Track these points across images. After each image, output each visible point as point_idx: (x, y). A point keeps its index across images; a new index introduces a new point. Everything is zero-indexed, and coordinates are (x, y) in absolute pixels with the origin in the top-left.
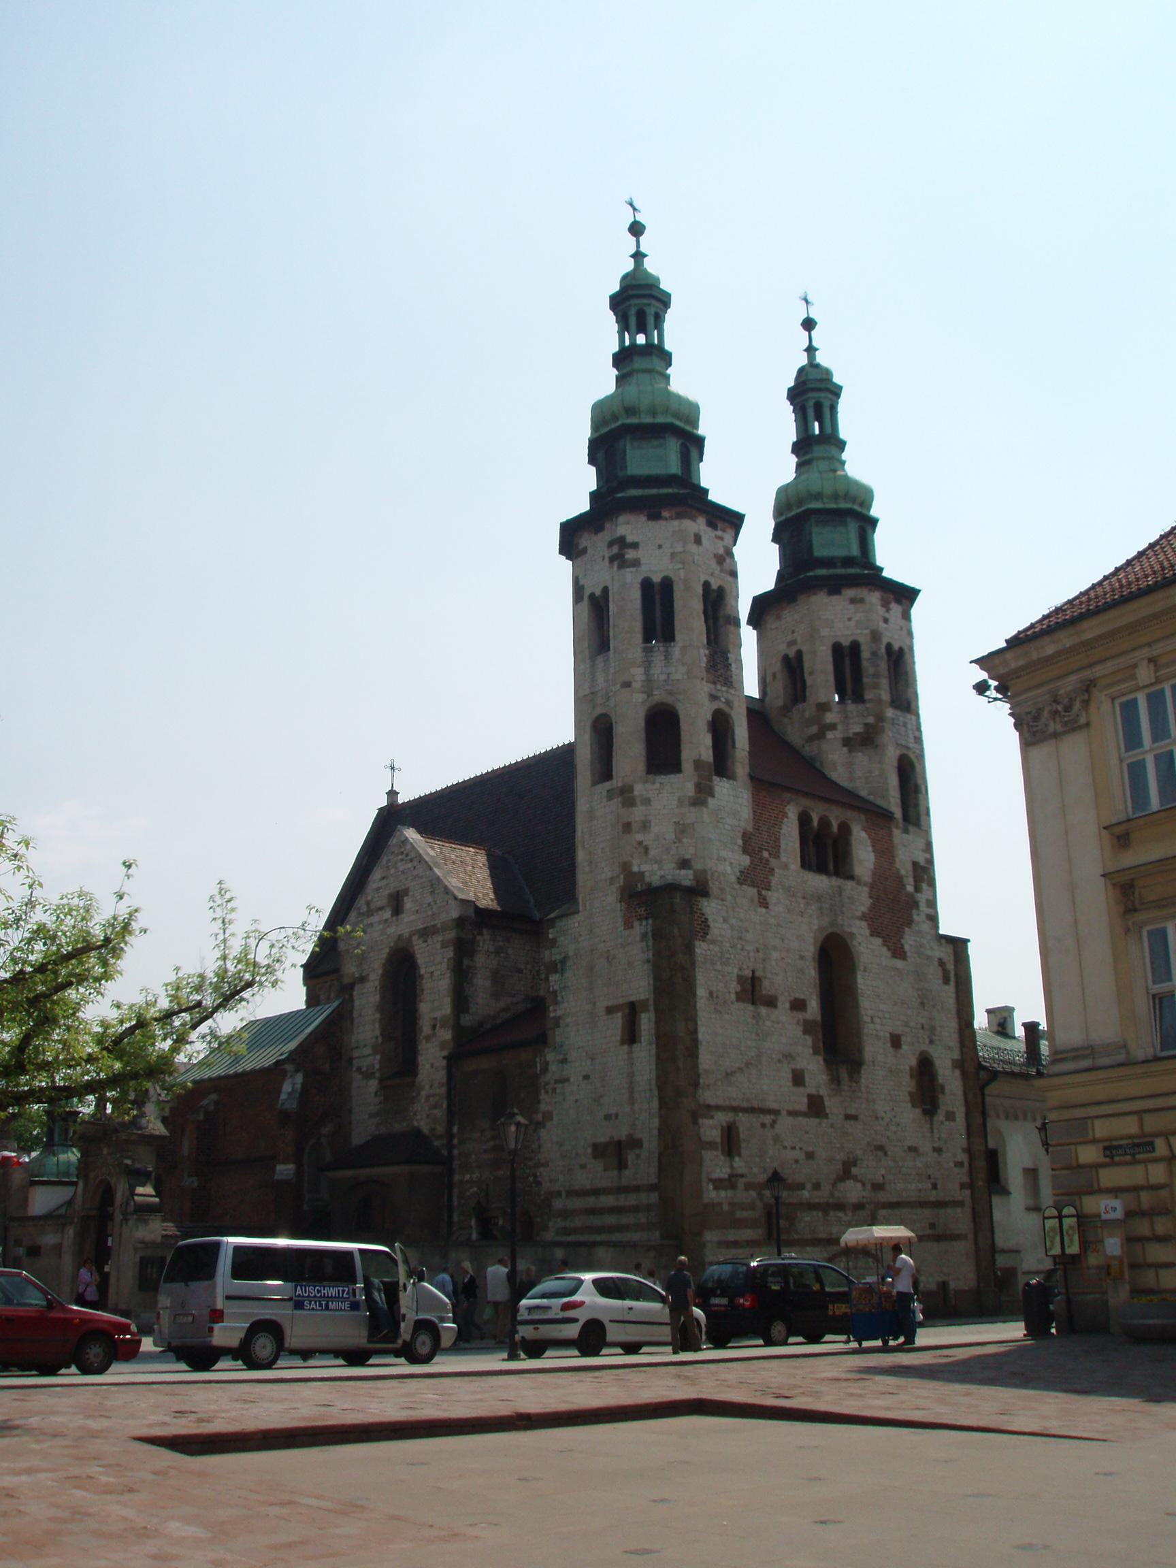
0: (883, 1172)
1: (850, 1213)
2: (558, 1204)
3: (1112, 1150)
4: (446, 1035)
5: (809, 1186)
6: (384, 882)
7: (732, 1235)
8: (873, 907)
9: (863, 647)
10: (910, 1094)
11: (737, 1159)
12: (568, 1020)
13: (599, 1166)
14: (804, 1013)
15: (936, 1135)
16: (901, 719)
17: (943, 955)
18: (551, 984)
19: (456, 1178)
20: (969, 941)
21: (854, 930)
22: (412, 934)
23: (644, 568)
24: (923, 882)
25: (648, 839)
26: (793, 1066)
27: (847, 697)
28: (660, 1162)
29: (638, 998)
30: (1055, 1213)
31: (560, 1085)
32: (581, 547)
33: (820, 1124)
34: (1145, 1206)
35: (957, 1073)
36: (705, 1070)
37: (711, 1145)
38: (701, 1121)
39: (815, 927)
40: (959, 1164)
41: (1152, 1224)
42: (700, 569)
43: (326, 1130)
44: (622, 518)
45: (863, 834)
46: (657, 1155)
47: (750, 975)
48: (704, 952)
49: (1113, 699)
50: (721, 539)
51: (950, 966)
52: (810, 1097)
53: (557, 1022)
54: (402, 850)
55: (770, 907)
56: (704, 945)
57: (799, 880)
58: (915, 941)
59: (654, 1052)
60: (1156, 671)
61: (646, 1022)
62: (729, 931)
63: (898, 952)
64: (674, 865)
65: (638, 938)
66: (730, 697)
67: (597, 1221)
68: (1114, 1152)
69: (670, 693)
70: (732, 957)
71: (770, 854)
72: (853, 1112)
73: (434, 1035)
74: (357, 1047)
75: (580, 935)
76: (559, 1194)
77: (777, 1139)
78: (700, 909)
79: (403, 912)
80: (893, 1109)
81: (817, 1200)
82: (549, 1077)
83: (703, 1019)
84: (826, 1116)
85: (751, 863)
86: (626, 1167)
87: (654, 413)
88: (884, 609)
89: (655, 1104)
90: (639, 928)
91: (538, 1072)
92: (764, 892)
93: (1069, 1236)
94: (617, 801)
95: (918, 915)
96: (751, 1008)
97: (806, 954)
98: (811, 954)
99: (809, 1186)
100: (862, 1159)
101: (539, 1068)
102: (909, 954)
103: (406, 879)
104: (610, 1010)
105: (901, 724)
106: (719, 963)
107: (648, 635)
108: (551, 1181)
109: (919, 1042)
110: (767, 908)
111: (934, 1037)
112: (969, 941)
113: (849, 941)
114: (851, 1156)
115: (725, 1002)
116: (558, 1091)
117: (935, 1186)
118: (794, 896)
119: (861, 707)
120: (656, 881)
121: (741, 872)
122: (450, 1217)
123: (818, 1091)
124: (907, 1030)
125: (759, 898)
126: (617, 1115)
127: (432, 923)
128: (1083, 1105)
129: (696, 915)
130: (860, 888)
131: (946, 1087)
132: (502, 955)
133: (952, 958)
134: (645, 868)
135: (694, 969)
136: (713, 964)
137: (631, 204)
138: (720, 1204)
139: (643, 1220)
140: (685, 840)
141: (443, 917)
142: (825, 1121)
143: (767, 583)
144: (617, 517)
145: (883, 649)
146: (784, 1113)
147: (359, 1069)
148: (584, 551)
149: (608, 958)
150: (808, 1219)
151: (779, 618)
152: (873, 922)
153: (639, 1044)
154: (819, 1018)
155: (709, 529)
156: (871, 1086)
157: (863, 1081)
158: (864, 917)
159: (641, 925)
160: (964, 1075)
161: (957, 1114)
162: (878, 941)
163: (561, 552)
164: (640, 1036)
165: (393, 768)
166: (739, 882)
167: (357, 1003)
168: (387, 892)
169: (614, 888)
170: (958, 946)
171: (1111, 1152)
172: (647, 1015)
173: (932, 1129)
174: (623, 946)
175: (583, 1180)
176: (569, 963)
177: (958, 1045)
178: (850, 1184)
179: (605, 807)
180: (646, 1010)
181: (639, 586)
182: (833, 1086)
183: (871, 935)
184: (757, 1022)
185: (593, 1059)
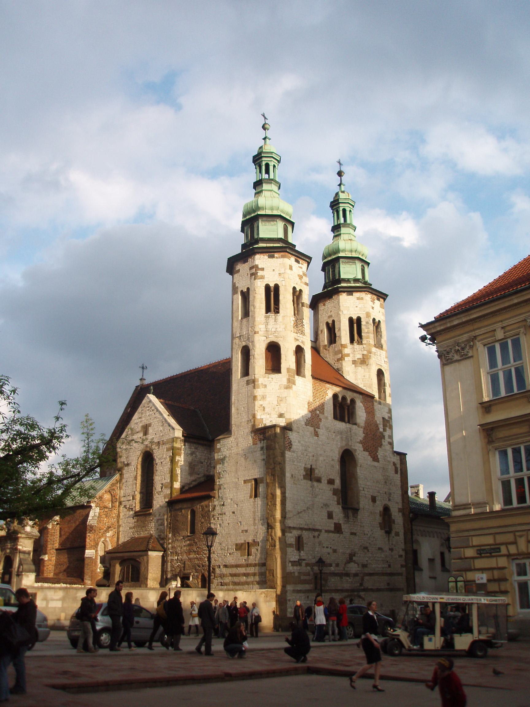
0: (367, 559)
1: (352, 578)
2: (218, 571)
3: (482, 552)
4: (169, 492)
5: (334, 565)
6: (140, 420)
7: (299, 587)
8: (365, 438)
9: (362, 320)
10: (380, 523)
11: (302, 552)
12: (225, 486)
13: (239, 553)
14: (333, 485)
15: (391, 543)
16: (379, 352)
17: (395, 461)
20: (407, 454)
21: (356, 448)
24: (387, 427)
25: (264, 403)
26: (328, 510)
27: (354, 342)
30: (453, 579)
31: (221, 516)
32: (237, 269)
33: (339, 536)
34: (496, 577)
35: (401, 514)
36: (289, 511)
37: (291, 545)
38: (286, 534)
39: (339, 446)
40: (401, 556)
41: (499, 585)
42: (291, 281)
43: (108, 534)
44: (257, 256)
45: (361, 404)
47: (310, 467)
48: (289, 456)
49: (484, 345)
50: (301, 268)
51: (398, 466)
52: (335, 524)
54: (149, 405)
55: (319, 436)
56: (289, 452)
57: (332, 424)
58: (383, 454)
60: (504, 333)
62: (301, 447)
63: (375, 459)
65: (259, 449)
66: (304, 340)
67: (236, 579)
68: (482, 552)
70: (302, 458)
71: (320, 412)
72: (355, 531)
73: (162, 491)
74: (124, 496)
75: (232, 447)
77: (320, 543)
78: (289, 437)
80: (372, 530)
81: (336, 572)
82: (215, 512)
83: (288, 487)
84: (342, 533)
85: (312, 416)
87: (272, 209)
88: (372, 303)
92: (317, 429)
93: (460, 590)
95: (384, 442)
96: (310, 482)
97: (335, 458)
98: (337, 458)
99: (334, 565)
100: (358, 553)
102: (380, 460)
103: (151, 419)
104: (245, 482)
105: (379, 355)
106: (296, 461)
107: (268, 310)
109: (384, 500)
110: (318, 437)
111: (391, 498)
112: (407, 454)
113: (354, 453)
114: (353, 551)
115: (298, 479)
117: (389, 566)
118: (330, 432)
119: (361, 346)
120: (268, 424)
121: (307, 420)
123: (339, 521)
124: (379, 494)
125: (314, 432)
127: (162, 440)
128: (467, 531)
129: (286, 439)
130: (359, 429)
131: (396, 521)
132: (194, 455)
133: (399, 462)
135: (285, 464)
136: (293, 462)
137: (264, 116)
138: (294, 572)
140: (282, 404)
142: (342, 535)
143: (319, 290)
145: (371, 321)
146: (323, 531)
148: (239, 271)
150: (333, 580)
151: (324, 305)
152: (364, 444)
154: (340, 488)
155: (296, 263)
156: (362, 519)
157: (359, 517)
158: (361, 442)
159: (261, 443)
160: (404, 515)
161: (400, 533)
162: (367, 453)
163: (227, 272)
165: (143, 368)
166: (306, 425)
168: (141, 425)
170: (402, 456)
171: (480, 552)
172: (263, 484)
173: (389, 539)
175: (231, 560)
176: (227, 459)
177: (401, 501)
178: (352, 565)
181: (264, 288)
182: (345, 519)
183: (364, 450)
184: (312, 490)
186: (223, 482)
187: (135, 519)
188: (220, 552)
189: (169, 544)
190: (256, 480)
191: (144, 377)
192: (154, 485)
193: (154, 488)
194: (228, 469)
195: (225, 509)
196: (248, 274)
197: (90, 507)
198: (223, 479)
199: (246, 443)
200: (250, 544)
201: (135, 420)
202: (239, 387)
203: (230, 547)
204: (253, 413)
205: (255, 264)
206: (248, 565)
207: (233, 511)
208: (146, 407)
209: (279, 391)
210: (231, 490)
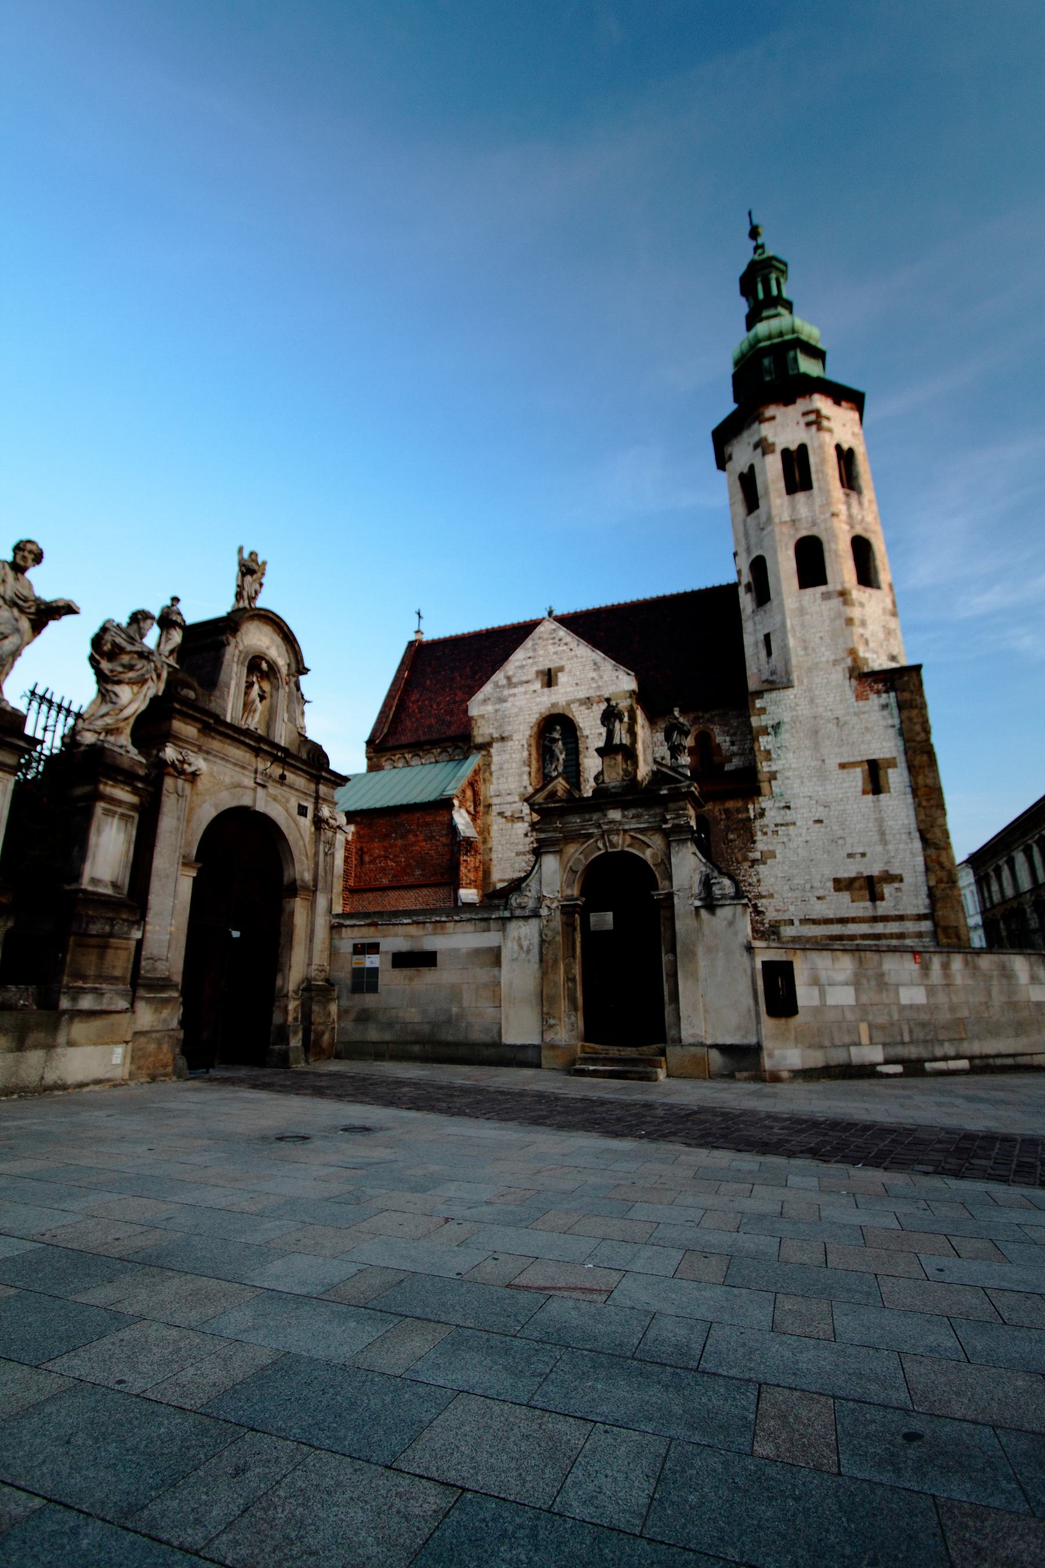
2: (787, 932)
6: (530, 661)
13: (845, 897)
22: (568, 704)
25: (867, 634)
28: (931, 894)
29: (882, 756)
31: (783, 828)
46: (926, 888)
53: (773, 776)
61: (897, 778)
65: (876, 708)
69: (866, 530)
76: (791, 922)
79: (557, 684)
82: (765, 821)
86: (882, 899)
89: (918, 845)
90: (875, 701)
91: (752, 817)
94: (836, 602)
101: (752, 815)
104: (843, 766)
108: (777, 911)
116: (779, 833)
126: (863, 855)
134: (868, 655)
144: (810, 396)
147: (501, 814)
148: (773, 418)
149: (838, 725)
153: (888, 794)
164: (889, 788)
165: (420, 617)
167: (495, 759)
168: (535, 669)
169: (839, 668)
172: (895, 770)
174: (855, 714)
176: (783, 728)
179: (820, 605)
180: (895, 766)
186: (781, 767)
187: (532, 836)
188: (789, 895)
191: (422, 629)
193: (582, 779)
194: (793, 743)
195: (789, 816)
197: (453, 805)
199: (838, 698)
200: (875, 879)
201: (517, 660)
202: (803, 603)
203: (817, 884)
204: (850, 646)
206: (875, 919)
207: (816, 818)
208: (547, 639)
209: (882, 617)
210: (805, 780)
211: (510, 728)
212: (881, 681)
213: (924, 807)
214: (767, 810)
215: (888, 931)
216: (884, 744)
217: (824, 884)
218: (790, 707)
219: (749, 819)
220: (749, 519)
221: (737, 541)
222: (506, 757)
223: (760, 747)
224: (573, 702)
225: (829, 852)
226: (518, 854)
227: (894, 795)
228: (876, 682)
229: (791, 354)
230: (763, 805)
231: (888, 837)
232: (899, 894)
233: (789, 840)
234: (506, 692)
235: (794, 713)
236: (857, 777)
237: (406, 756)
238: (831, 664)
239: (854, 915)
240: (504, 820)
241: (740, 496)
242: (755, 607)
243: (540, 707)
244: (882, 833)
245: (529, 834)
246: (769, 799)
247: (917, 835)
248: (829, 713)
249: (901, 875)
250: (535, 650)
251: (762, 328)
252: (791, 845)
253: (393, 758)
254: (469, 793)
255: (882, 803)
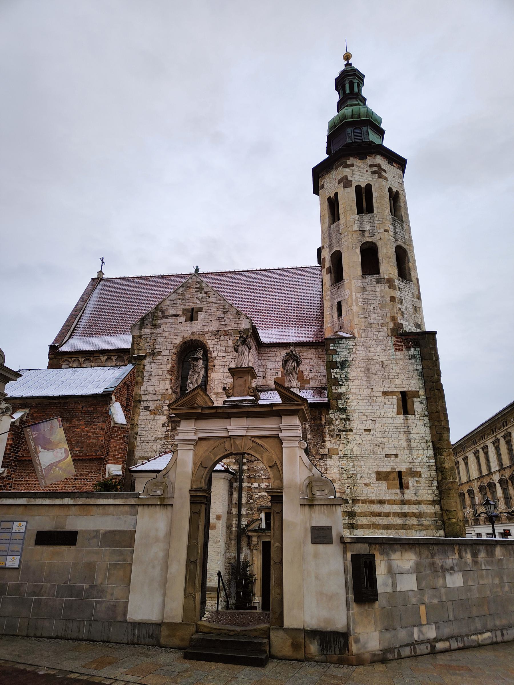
6: (180, 301)
12: (347, 396)
13: (383, 485)
18: (332, 374)
19: (245, 485)
23: (389, 182)
25: (403, 308)
29: (410, 390)
31: (344, 433)
44: (378, 157)
46: (436, 482)
59: (427, 421)
64: (414, 325)
65: (407, 357)
75: (357, 350)
79: (197, 320)
86: (408, 488)
89: (431, 451)
91: (324, 424)
104: (385, 394)
116: (342, 436)
120: (408, 331)
122: (240, 510)
126: (396, 456)
134: (402, 323)
139: (427, 523)
141: (235, 327)
144: (375, 156)
148: (352, 165)
165: (103, 263)
168: (183, 307)
172: (419, 400)
185: (372, 421)
186: (345, 391)
187: (168, 426)
189: (244, 464)
190: (404, 394)
192: (209, 383)
193: (208, 387)
194: (353, 375)
196: (367, 171)
197: (111, 400)
198: (343, 387)
199: (383, 348)
200: (403, 474)
204: (393, 315)
205: (377, 163)
206: (403, 502)
207: (367, 428)
209: (412, 299)
211: (159, 346)
212: (411, 340)
213: (436, 426)
214: (334, 419)
215: (410, 511)
216: (413, 382)
217: (370, 475)
218: (353, 351)
219: (321, 425)
220: (332, 226)
221: (323, 239)
222: (155, 367)
223: (331, 375)
224: (207, 332)
225: (374, 452)
226: (157, 439)
227: (417, 416)
228: (407, 339)
229: (365, 129)
230: (332, 416)
231: (413, 445)
232: (419, 485)
233: (348, 442)
234: (159, 321)
235: (354, 355)
236: (394, 401)
237: (80, 359)
238: (380, 325)
239: (389, 498)
240: (149, 412)
241: (327, 212)
242: (332, 282)
243: (183, 334)
244: (409, 442)
245: (166, 425)
246: (336, 412)
247: (431, 445)
248: (377, 358)
249: (420, 471)
250: (183, 294)
251: (347, 111)
252: (350, 446)
253: (70, 360)
254: (125, 392)
255: (409, 421)
